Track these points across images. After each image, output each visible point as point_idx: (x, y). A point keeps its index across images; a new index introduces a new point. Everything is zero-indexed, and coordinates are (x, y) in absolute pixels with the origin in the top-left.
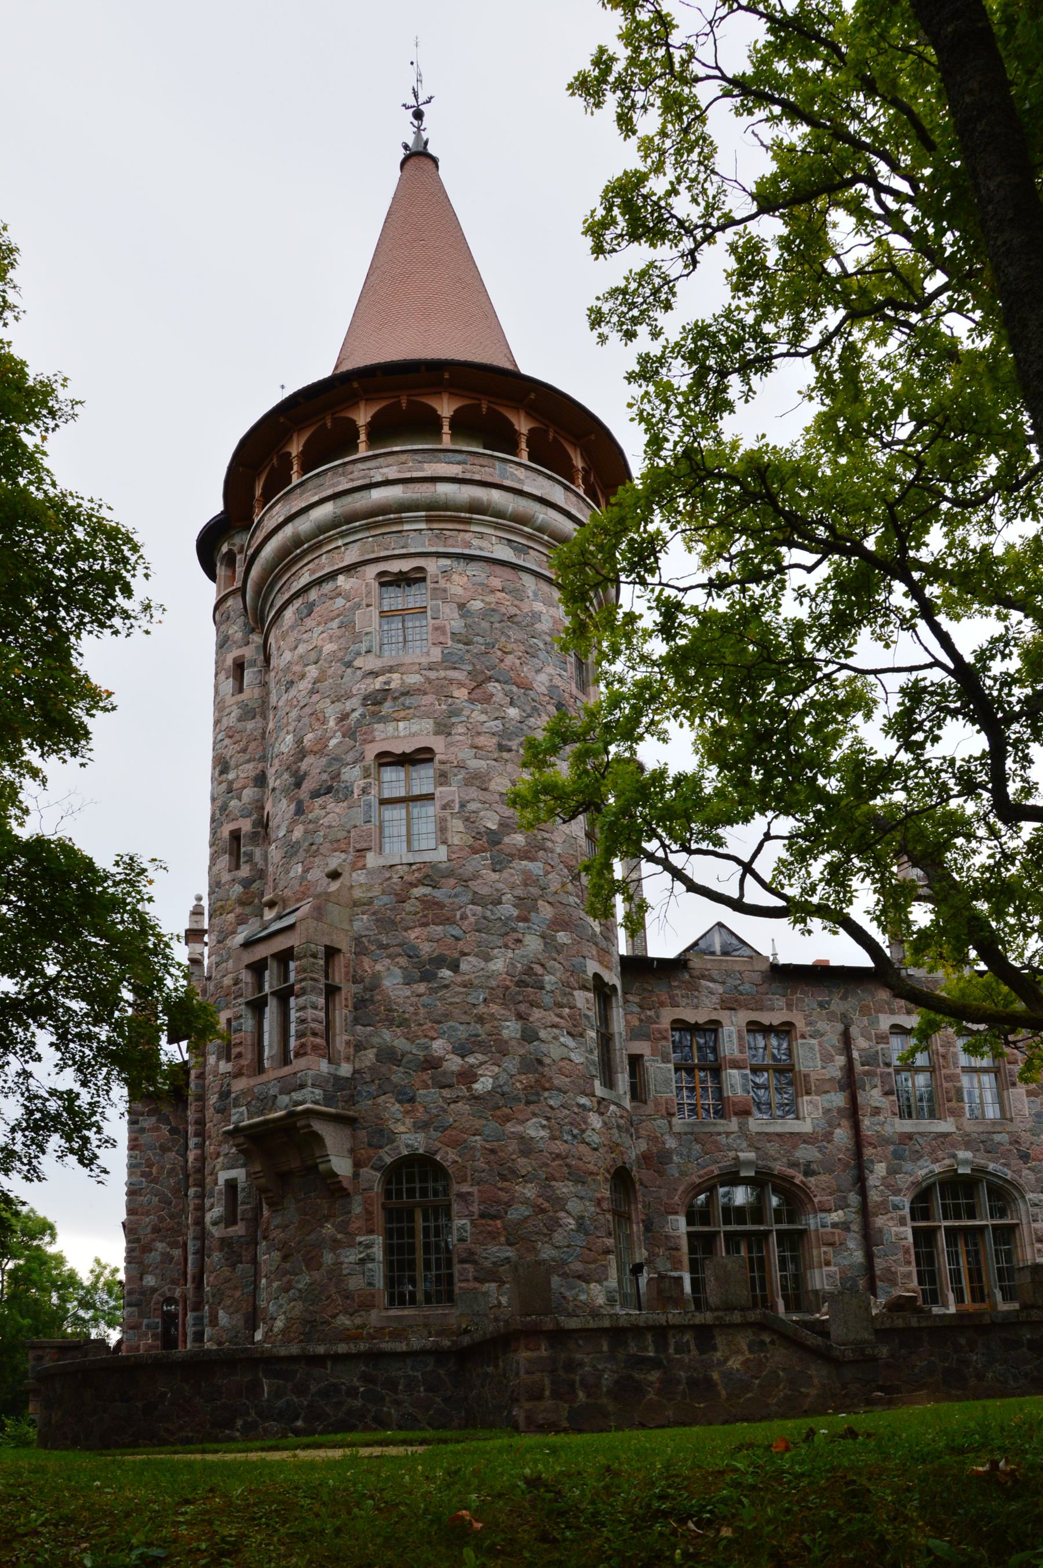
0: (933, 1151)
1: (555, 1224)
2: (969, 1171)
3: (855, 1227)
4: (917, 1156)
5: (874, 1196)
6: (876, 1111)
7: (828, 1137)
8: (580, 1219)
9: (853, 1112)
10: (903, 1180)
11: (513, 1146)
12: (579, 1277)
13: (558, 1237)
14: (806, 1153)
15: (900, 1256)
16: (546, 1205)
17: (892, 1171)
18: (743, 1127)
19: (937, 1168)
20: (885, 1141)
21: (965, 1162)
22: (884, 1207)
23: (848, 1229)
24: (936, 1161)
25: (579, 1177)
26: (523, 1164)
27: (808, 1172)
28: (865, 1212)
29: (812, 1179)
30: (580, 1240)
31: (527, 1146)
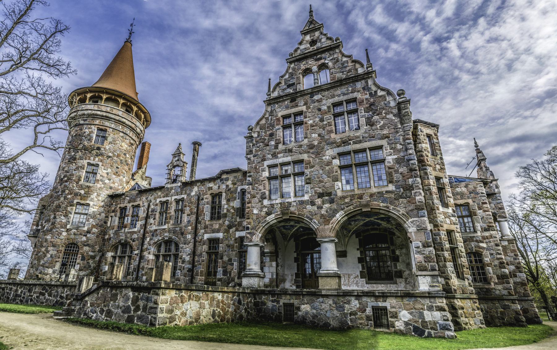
0: (161, 233)
1: (45, 256)
2: (167, 239)
3: (139, 255)
4: (157, 235)
5: (145, 247)
6: (151, 224)
7: (139, 231)
8: (51, 256)
9: (145, 225)
10: (152, 242)
11: (44, 240)
12: (47, 267)
13: (45, 259)
14: (135, 236)
15: (147, 263)
16: (45, 252)
17: (151, 240)
18: (125, 230)
19: (160, 238)
20: (151, 231)
21: (166, 236)
22: (147, 249)
23: (138, 255)
24: (160, 236)
25: (54, 246)
26: (45, 244)
27: (134, 241)
28: (142, 251)
29: (134, 243)
30: (51, 259)
31: (46, 240)
